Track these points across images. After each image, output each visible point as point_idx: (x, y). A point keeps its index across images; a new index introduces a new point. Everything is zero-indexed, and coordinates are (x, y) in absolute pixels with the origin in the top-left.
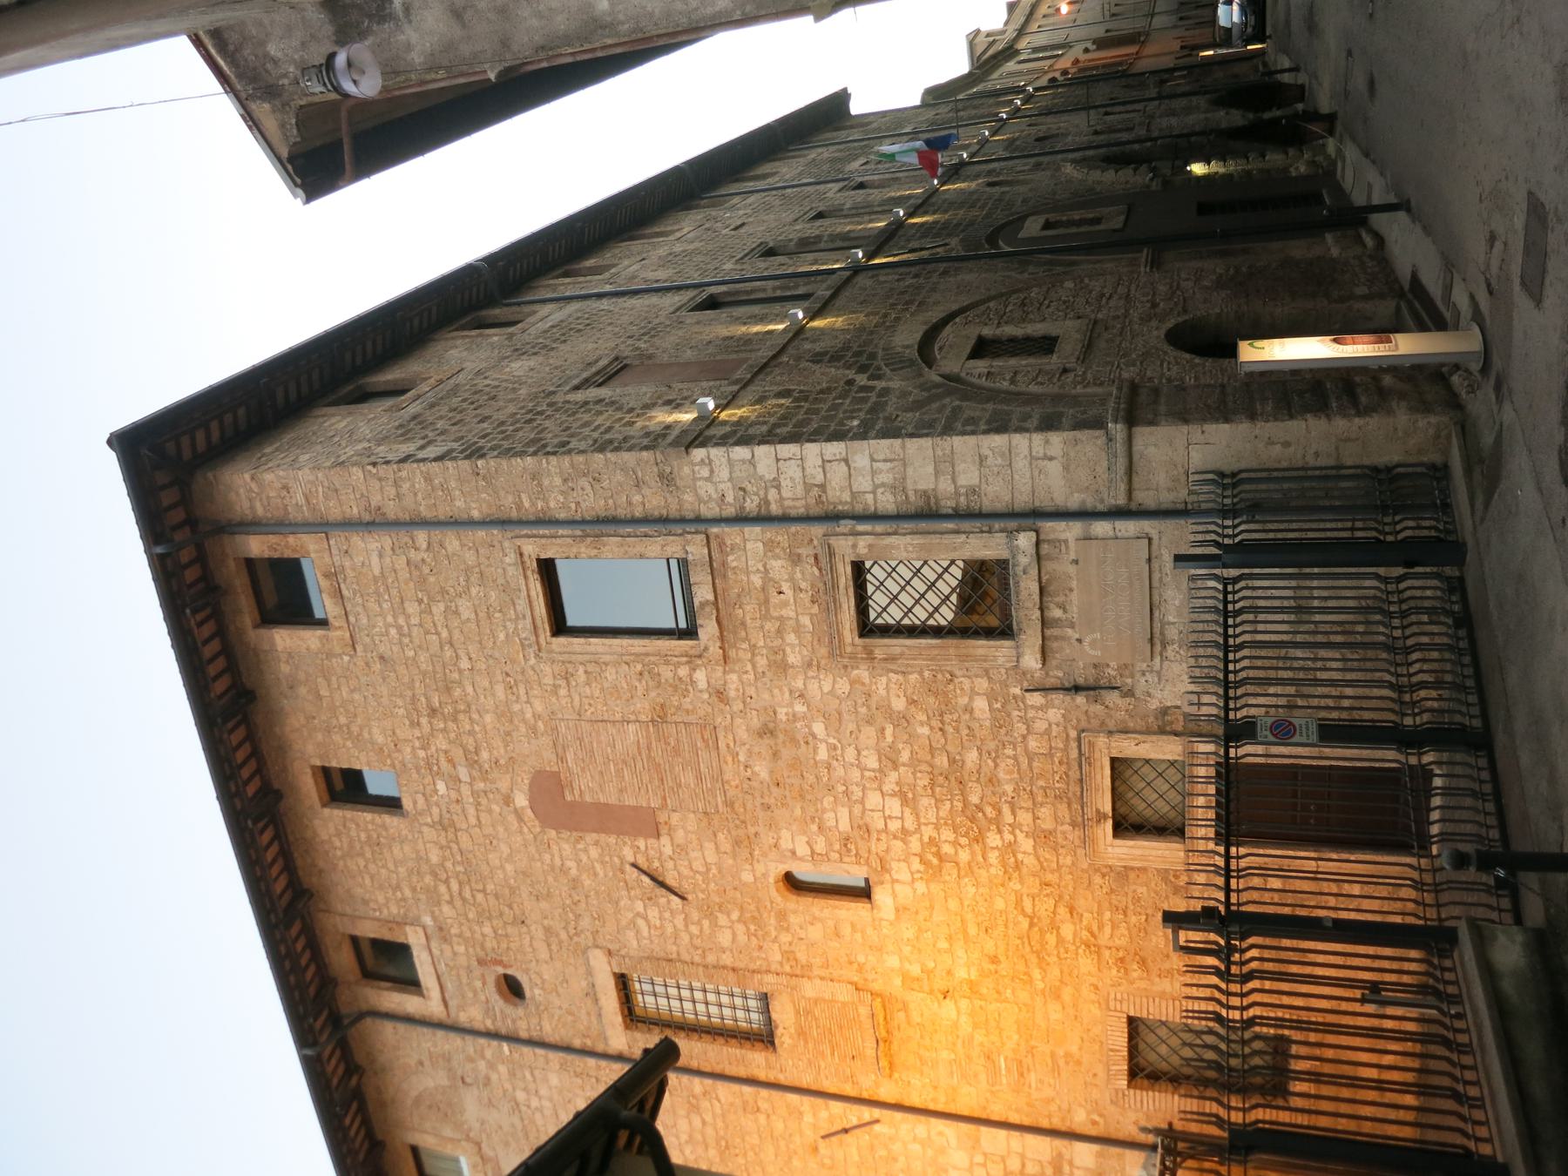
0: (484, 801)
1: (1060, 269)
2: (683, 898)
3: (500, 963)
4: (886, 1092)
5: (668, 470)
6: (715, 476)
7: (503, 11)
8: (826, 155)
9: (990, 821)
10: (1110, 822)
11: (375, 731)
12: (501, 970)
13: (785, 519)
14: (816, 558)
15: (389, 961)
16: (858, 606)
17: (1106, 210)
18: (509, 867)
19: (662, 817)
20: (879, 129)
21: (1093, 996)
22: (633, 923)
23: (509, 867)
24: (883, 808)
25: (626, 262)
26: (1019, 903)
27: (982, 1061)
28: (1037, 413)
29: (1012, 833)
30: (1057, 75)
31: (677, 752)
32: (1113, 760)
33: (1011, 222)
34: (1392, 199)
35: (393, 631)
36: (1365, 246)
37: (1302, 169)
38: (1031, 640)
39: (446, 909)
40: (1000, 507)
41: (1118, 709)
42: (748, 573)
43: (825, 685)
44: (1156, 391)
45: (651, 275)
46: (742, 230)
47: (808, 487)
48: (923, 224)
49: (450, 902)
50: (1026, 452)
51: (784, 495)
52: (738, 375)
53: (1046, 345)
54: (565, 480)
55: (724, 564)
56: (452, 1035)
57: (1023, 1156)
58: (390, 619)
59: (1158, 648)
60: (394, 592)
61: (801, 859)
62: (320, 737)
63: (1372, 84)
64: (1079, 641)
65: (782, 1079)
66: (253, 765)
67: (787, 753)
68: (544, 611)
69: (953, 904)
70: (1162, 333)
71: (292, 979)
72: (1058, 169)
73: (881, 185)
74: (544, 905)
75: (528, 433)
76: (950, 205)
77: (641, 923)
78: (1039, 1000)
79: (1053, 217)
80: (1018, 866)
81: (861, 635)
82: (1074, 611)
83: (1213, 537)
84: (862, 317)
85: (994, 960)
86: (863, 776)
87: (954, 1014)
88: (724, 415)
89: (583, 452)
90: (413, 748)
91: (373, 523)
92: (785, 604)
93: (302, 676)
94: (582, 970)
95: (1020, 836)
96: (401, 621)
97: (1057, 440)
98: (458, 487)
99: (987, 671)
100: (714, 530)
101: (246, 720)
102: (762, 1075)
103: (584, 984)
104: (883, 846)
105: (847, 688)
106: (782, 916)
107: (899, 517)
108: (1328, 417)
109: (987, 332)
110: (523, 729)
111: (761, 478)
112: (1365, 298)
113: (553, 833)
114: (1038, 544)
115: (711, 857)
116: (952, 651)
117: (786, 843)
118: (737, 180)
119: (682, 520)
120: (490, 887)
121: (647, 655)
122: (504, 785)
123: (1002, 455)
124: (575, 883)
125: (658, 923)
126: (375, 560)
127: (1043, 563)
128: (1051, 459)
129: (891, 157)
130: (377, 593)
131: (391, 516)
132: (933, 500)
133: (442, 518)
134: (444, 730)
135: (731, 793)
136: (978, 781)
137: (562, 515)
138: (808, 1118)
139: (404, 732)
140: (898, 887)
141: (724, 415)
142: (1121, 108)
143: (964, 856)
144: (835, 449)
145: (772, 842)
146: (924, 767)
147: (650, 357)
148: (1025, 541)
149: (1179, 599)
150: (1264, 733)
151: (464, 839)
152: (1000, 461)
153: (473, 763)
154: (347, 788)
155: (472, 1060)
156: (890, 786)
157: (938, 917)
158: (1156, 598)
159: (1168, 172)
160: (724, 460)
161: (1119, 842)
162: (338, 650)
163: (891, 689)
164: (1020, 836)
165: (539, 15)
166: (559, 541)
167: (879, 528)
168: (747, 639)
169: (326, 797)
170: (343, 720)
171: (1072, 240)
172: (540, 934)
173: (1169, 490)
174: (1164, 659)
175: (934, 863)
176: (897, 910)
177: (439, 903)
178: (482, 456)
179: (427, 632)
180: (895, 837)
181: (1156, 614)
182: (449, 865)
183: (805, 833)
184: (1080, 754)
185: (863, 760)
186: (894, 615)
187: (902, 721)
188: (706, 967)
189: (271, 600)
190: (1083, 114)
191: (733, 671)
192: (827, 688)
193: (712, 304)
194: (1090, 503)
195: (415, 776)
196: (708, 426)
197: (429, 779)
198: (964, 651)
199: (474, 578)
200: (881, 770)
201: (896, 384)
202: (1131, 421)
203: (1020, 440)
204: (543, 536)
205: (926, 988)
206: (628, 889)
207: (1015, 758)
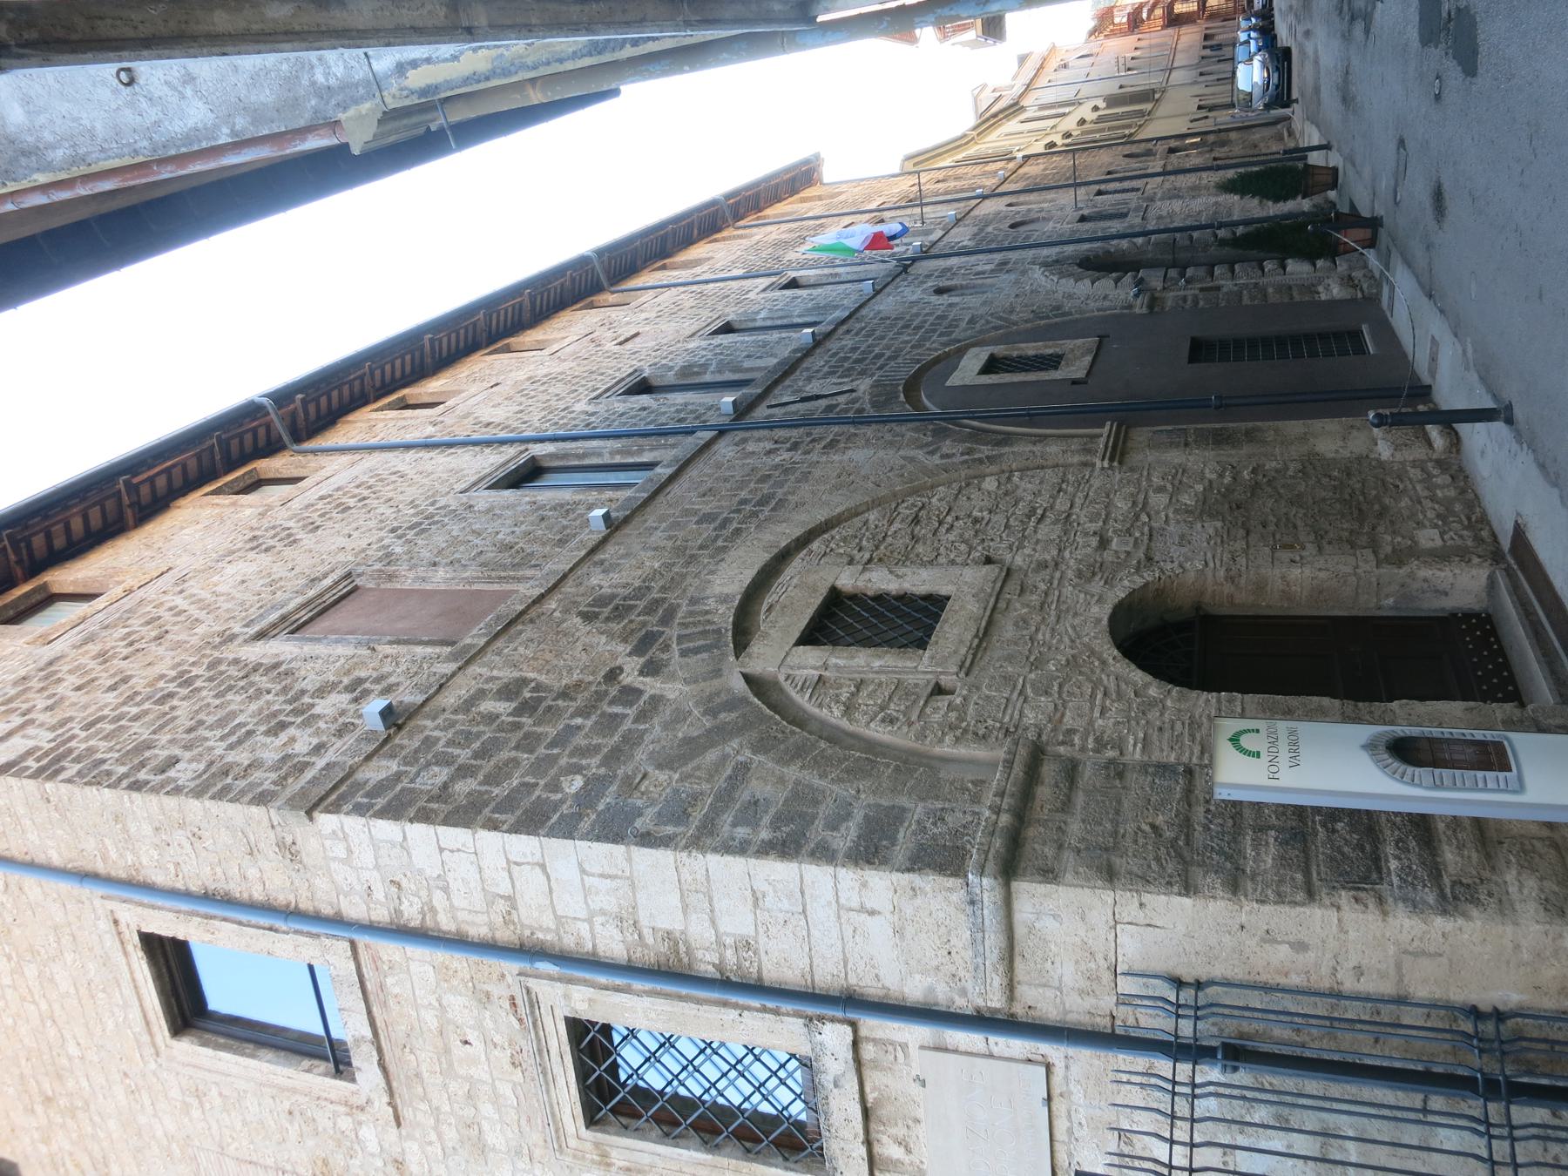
1: (985, 451)
5: (289, 840)
6: (357, 857)
8: (773, 236)
13: (459, 942)
16: (582, 1074)
17: (1069, 344)
28: (864, 798)
30: (1059, 140)
33: (947, 355)
34: (1488, 403)
36: (1430, 444)
37: (1336, 291)
44: (1071, 770)
45: (487, 414)
46: (629, 346)
47: (491, 898)
50: (830, 896)
51: (456, 904)
55: (382, 987)
63: (1438, 196)
72: (1024, 272)
75: (141, 731)
79: (1000, 350)
89: (177, 790)
97: (881, 885)
100: (362, 940)
107: (630, 969)
108: (1381, 900)
109: (847, 580)
111: (420, 872)
112: (1440, 556)
114: (855, 1044)
118: (664, 267)
119: (316, 918)
121: (294, 1091)
123: (790, 896)
127: (867, 1073)
128: (872, 913)
132: (682, 949)
137: (159, 879)
142: (1117, 185)
144: (524, 845)
152: (785, 905)
167: (603, 979)
191: (410, 1137)
193: (527, 475)
194: (943, 995)
199: (66, 940)
201: (672, 689)
202: (1009, 869)
203: (818, 876)
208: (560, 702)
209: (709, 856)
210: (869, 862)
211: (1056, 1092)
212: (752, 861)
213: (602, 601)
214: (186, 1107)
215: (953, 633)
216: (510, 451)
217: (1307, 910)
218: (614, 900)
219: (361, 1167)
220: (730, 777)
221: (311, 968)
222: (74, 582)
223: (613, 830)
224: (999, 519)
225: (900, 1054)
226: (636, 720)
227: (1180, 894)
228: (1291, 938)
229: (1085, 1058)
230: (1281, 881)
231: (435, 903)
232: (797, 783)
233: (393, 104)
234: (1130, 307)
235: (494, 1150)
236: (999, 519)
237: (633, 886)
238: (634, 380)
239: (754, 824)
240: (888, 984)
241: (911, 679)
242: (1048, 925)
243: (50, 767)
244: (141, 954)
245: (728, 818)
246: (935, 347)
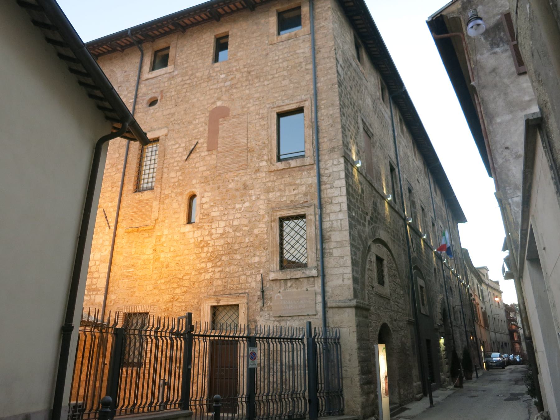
0: (218, 91)
1: (407, 290)
2: (186, 160)
3: (162, 98)
4: (120, 231)
5: (336, 150)
6: (334, 167)
7: (495, 86)
8: (443, 213)
9: (216, 264)
10: (215, 304)
11: (242, 53)
12: (159, 98)
13: (320, 191)
15: (161, 60)
17: (427, 307)
18: (195, 100)
19: (214, 152)
20: (453, 233)
21: (155, 300)
22: (177, 143)
23: (195, 100)
24: (219, 227)
25: (405, 141)
26: (188, 274)
27: (132, 263)
28: (359, 276)
29: (212, 271)
30: (473, 297)
31: (238, 156)
32: (237, 306)
33: (422, 275)
34: (434, 403)
35: (277, 58)
38: (280, 275)
39: (180, 79)
40: (326, 264)
42: (300, 178)
43: (262, 206)
45: (401, 149)
46: (417, 182)
47: (331, 198)
48: (421, 244)
49: (182, 80)
52: (368, 175)
53: (381, 282)
54: (331, 115)
55: (304, 170)
56: (136, 82)
57: (99, 278)
58: (281, 57)
59: (278, 319)
60: (291, 58)
61: (201, 199)
62: (239, 34)
63: (474, 397)
64: (280, 292)
65: (124, 195)
66: (229, 11)
67: (238, 193)
69: (186, 252)
70: (387, 322)
71: (154, 26)
72: (441, 293)
73: (434, 232)
74: (183, 112)
75: (347, 102)
76: (428, 255)
77: (177, 146)
78: (153, 282)
79: (424, 289)
80: (200, 274)
81: (280, 218)
83: (318, 335)
84: (389, 220)
85: (167, 266)
88: (355, 170)
90: (236, 66)
91: (314, 50)
92: (290, 191)
94: (160, 126)
95: (211, 274)
96: (281, 61)
97: (350, 282)
98: (328, 77)
99: (268, 261)
100: (315, 167)
101: (244, 8)
102: (125, 188)
103: (155, 127)
104: (206, 227)
106: (181, 194)
108: (359, 374)
109: (385, 262)
110: (244, 103)
111: (334, 182)
112: (399, 394)
113: (208, 115)
114: (313, 277)
115: (201, 169)
116: (275, 249)
117: (206, 194)
119: (318, 156)
120: (188, 94)
121: (271, 145)
122: (224, 97)
123: (344, 264)
124: (190, 123)
125: (177, 152)
126: (301, 51)
128: (343, 281)
129: (444, 235)
130: (290, 52)
131: (317, 56)
133: (317, 73)
134: (243, 77)
135: (224, 175)
136: (230, 259)
137: (319, 114)
138: (110, 204)
139: (241, 63)
140: (192, 233)
141: (355, 170)
142: (462, 317)
143: (203, 255)
144: (345, 207)
145: (207, 189)
146: (234, 241)
147: (374, 147)
148: (314, 272)
149: (296, 325)
150: (251, 349)
151: (205, 84)
152: (342, 263)
153: (231, 86)
154: (221, 44)
155: (127, 89)
156: (227, 229)
158: (295, 318)
159: (441, 331)
160: (340, 169)
161: (209, 307)
162: (270, 39)
163: (261, 228)
164: (211, 274)
165: (494, 98)
166: (310, 113)
167: (318, 223)
168: (277, 179)
169: (218, 37)
170: (245, 42)
171: (417, 296)
172: (172, 111)
173: (333, 321)
174: (274, 321)
175: (201, 245)
176: (184, 233)
177: (182, 76)
178: (339, 86)
179: (277, 70)
180: (209, 231)
181: (290, 318)
182: (196, 79)
183: (210, 201)
184: (240, 294)
185: (236, 220)
186: (287, 229)
188: (162, 168)
189: (286, 16)
190: (460, 304)
191: (266, 174)
192: (261, 207)
193: (392, 170)
194: (328, 294)
195: (227, 67)
196: (351, 164)
197: (225, 71)
199: (296, 85)
200: (233, 226)
201: (367, 229)
202: (357, 307)
203: (349, 270)
204: (311, 108)
205: (157, 244)
206: (189, 141)
207: (238, 271)
213: (376, 206)
214: (259, 114)
215: (379, 288)
216: (395, 162)
222: (362, 55)
224: (396, 296)
233: (503, 201)
234: (435, 323)
236: (396, 296)
238: (411, 188)
241: (374, 281)
242: (346, 315)
243: (340, 84)
244: (297, 106)
246: (424, 271)
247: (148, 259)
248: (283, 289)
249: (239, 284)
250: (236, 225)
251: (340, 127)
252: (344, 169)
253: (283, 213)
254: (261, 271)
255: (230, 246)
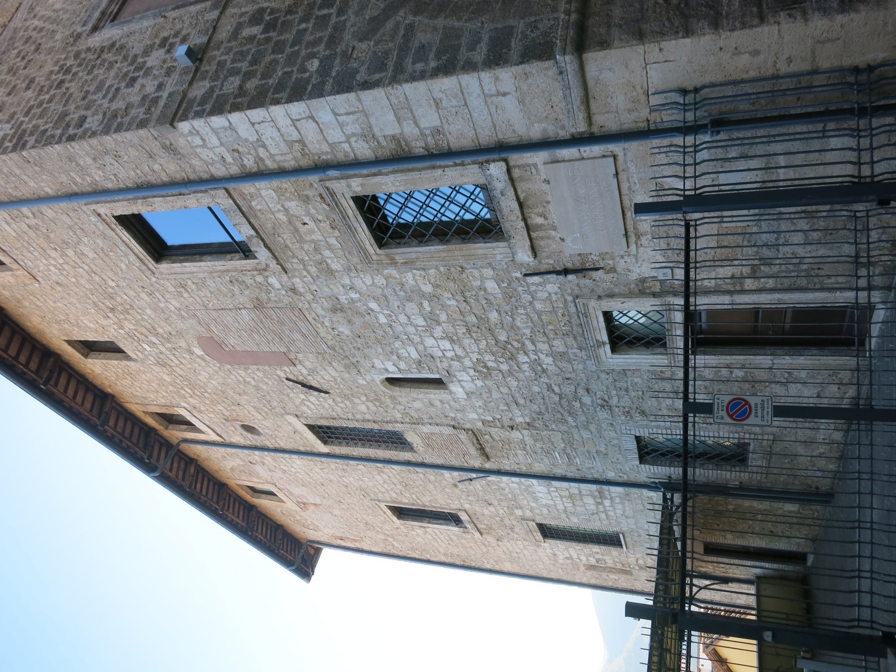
9: (518, 349)
10: (608, 348)
13: (281, 173)
14: (321, 195)
16: (369, 223)
19: (292, 356)
26: (549, 388)
31: (282, 324)
35: (52, 268)
39: (191, 400)
41: (603, 281)
43: (364, 281)
47: (290, 144)
49: (191, 397)
50: (478, 91)
51: (272, 152)
54: (94, 159)
55: (251, 207)
59: (633, 239)
60: (34, 245)
67: (357, 320)
68: (140, 249)
69: (505, 390)
74: (245, 397)
75: (56, 108)
78: (575, 431)
80: (544, 371)
82: (554, 217)
86: (417, 330)
87: (521, 437)
89: (94, 134)
92: (312, 232)
93: (19, 296)
97: (506, 76)
100: (231, 186)
105: (385, 282)
108: (804, 13)
111: (246, 140)
113: (229, 367)
114: (509, 171)
115: (334, 374)
117: (378, 364)
119: (201, 181)
121: (228, 271)
123: (456, 97)
124: (258, 388)
127: (517, 184)
132: (403, 143)
135: (329, 343)
136: (502, 328)
140: (462, 383)
143: (504, 367)
144: (297, 108)
146: (459, 323)
152: (454, 103)
153: (157, 335)
157: (495, 395)
160: (208, 129)
161: (614, 356)
162: (27, 282)
164: (542, 357)
167: (365, 171)
168: (294, 256)
170: (63, 318)
172: (251, 409)
176: (467, 394)
178: (23, 147)
180: (452, 359)
182: (178, 381)
183: (389, 360)
187: (432, 298)
192: (369, 282)
194: (553, 132)
197: (136, 344)
198: (465, 252)
199: (79, 232)
200: (428, 326)
203: (469, 80)
204: (109, 202)
207: (527, 314)
208: (289, 17)
209: (404, 85)
210: (497, 65)
211: (620, 169)
212: (430, 82)
217: (759, 29)
218: (358, 126)
219: (276, 296)
220: (404, 35)
221: (210, 208)
223: (345, 85)
225: (534, 170)
226: (338, 15)
227: (683, 37)
228: (750, 49)
229: (635, 147)
230: (744, 15)
231: (261, 155)
232: (445, 28)
235: (337, 271)
237: (366, 115)
239: (426, 60)
240: (520, 133)
242: (607, 75)
243: (20, 144)
244: (120, 227)
245: (409, 60)
247: (532, 436)
248: (553, 233)
249: (556, 313)
250: (426, 321)
251: (107, 139)
252: (202, 120)
253: (368, 243)
254: (518, 275)
255: (475, 329)
